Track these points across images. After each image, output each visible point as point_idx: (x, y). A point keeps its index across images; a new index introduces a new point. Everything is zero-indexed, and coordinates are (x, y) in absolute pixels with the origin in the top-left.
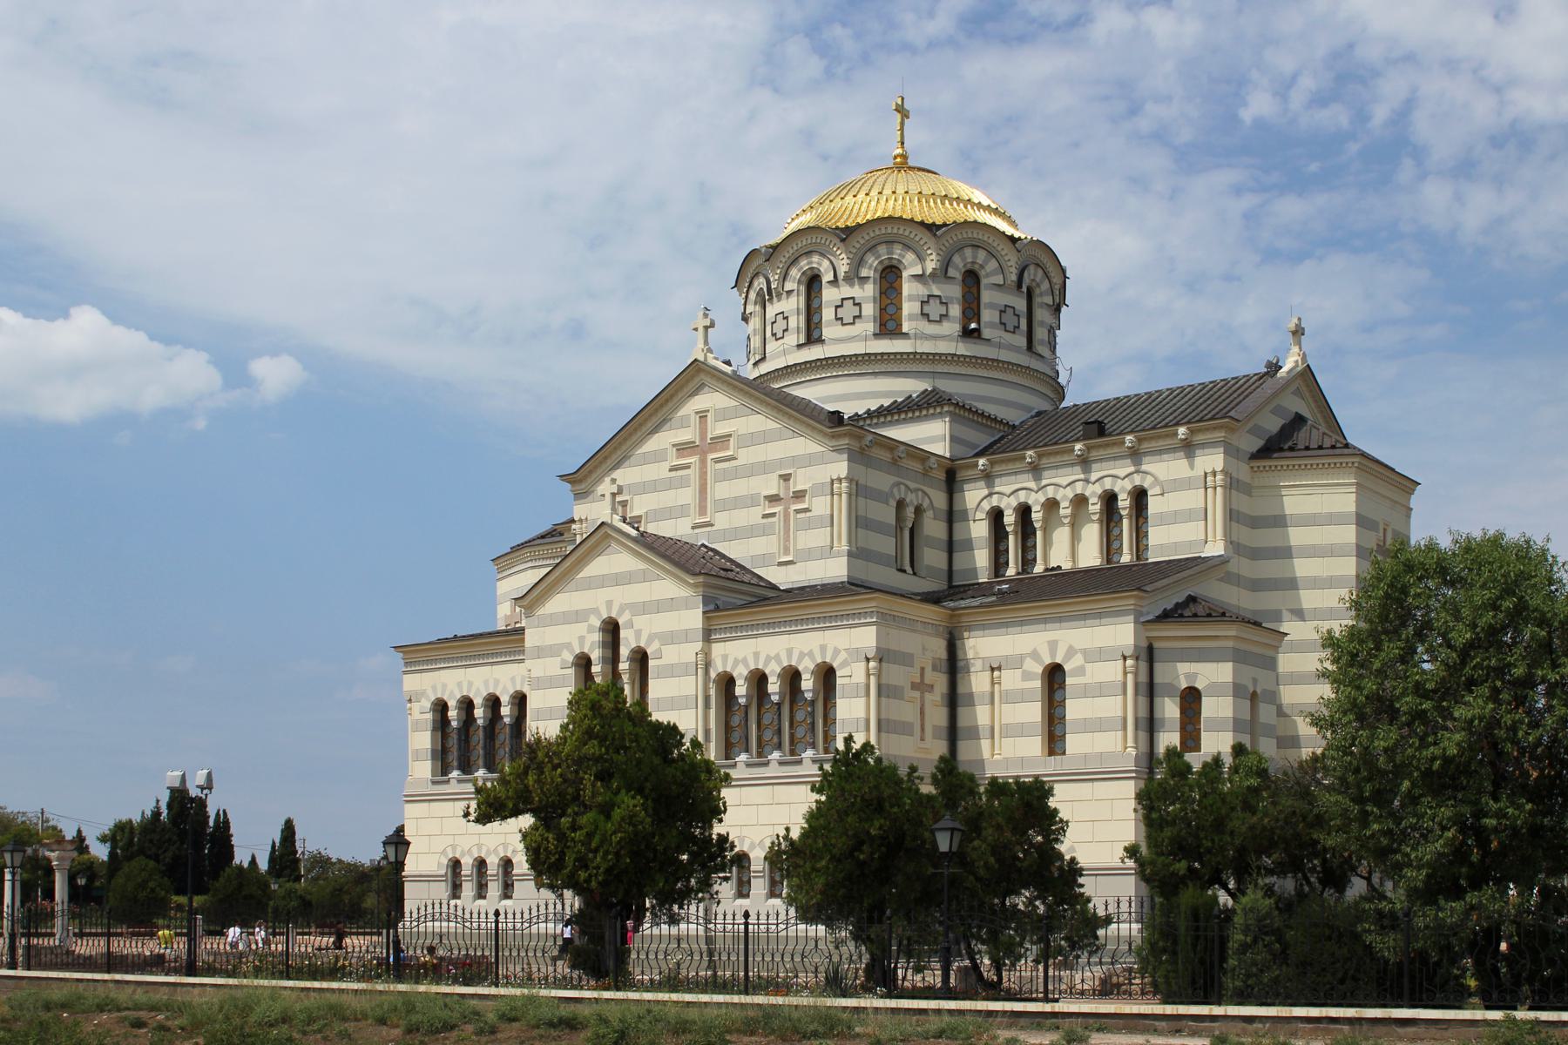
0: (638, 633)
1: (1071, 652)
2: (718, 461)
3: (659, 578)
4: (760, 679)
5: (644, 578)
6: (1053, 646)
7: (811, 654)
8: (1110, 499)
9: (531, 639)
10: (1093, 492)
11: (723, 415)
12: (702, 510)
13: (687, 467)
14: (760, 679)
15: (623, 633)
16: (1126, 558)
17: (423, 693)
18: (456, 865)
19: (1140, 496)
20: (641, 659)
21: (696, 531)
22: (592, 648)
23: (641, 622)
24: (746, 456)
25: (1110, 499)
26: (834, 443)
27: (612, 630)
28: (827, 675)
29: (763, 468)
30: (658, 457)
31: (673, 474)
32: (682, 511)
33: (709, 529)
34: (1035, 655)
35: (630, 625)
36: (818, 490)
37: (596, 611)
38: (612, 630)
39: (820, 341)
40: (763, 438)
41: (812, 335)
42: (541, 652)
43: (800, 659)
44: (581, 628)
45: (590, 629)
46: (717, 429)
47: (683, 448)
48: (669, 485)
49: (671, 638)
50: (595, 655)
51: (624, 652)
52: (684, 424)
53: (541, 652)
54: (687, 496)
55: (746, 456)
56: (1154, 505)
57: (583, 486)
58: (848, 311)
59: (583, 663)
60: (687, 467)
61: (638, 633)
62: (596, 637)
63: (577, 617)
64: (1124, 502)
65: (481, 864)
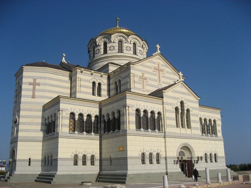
0: (188, 105)
5: (188, 94)
9: (165, 99)
11: (162, 65)
12: (160, 82)
15: (185, 105)
18: (143, 154)
20: (188, 111)
21: (159, 85)
23: (188, 103)
24: (167, 75)
27: (182, 103)
32: (155, 81)
33: (161, 86)
35: (186, 103)
38: (182, 103)
39: (122, 52)
40: (170, 73)
41: (121, 50)
42: (168, 104)
46: (161, 67)
48: (153, 74)
49: (194, 108)
50: (180, 108)
51: (186, 109)
52: (155, 63)
53: (168, 104)
54: (156, 78)
55: (167, 75)
57: (133, 66)
59: (177, 109)
61: (188, 105)
63: (175, 98)
65: (151, 154)
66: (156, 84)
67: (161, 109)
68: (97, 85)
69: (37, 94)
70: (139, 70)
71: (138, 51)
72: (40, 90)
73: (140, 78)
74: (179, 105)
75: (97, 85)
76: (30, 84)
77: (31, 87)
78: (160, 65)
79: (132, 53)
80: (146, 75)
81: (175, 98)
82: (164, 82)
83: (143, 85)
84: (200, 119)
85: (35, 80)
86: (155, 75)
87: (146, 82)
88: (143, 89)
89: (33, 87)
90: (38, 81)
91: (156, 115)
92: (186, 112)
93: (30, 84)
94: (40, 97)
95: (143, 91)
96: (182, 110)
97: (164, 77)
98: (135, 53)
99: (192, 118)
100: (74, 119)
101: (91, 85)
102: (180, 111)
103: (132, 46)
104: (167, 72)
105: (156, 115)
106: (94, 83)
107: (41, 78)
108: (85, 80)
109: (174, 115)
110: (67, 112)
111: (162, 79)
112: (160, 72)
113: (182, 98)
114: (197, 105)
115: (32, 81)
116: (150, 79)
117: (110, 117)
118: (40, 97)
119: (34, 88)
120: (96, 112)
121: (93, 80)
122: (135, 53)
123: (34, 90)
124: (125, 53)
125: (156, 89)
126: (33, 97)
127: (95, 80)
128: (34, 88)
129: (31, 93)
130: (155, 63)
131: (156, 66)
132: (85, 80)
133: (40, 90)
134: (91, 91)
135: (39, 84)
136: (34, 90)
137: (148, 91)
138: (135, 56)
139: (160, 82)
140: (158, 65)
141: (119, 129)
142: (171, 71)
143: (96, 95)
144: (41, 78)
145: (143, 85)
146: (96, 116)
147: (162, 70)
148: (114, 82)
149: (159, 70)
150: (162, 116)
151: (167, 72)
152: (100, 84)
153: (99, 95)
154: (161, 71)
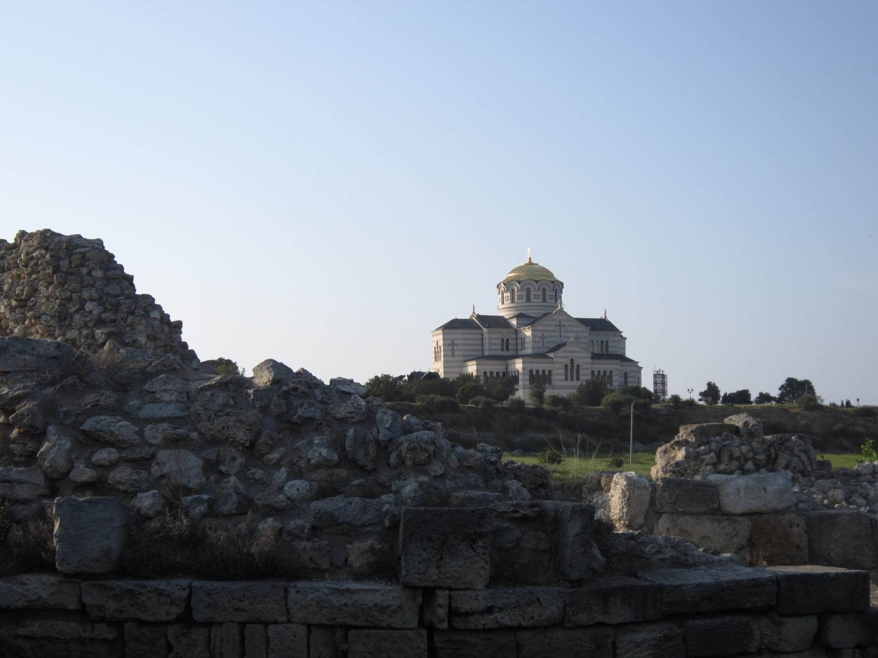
1: (628, 371)
5: (579, 352)
6: (626, 369)
8: (602, 342)
9: (555, 360)
10: (600, 340)
11: (564, 320)
12: (560, 337)
15: (575, 361)
16: (605, 352)
17: (527, 368)
19: (607, 342)
20: (578, 366)
25: (602, 342)
27: (572, 361)
28: (611, 372)
29: (572, 332)
30: (551, 325)
34: (623, 371)
36: (584, 337)
38: (572, 361)
42: (558, 363)
44: (567, 359)
46: (563, 323)
47: (556, 326)
48: (553, 331)
50: (570, 364)
51: (575, 365)
53: (558, 363)
54: (557, 334)
55: (569, 329)
56: (610, 344)
59: (566, 366)
62: (570, 361)
64: (605, 343)
66: (556, 340)
68: (505, 341)
69: (456, 353)
71: (547, 297)
73: (540, 337)
74: (569, 363)
76: (449, 345)
77: (450, 348)
78: (562, 321)
79: (541, 300)
80: (546, 334)
82: (564, 337)
84: (593, 372)
85: (453, 341)
86: (556, 331)
88: (543, 346)
90: (456, 342)
91: (547, 373)
92: (575, 367)
93: (449, 345)
97: (564, 331)
98: (544, 300)
99: (581, 372)
100: (486, 376)
101: (500, 342)
102: (569, 367)
103: (540, 293)
105: (547, 373)
106: (502, 339)
107: (457, 339)
108: (494, 339)
109: (563, 371)
110: (482, 372)
111: (563, 334)
112: (562, 328)
114: (589, 360)
115: (450, 342)
116: (550, 337)
117: (513, 374)
119: (453, 348)
120: (503, 369)
121: (502, 337)
122: (544, 300)
125: (557, 344)
126: (453, 356)
127: (503, 337)
128: (453, 348)
129: (450, 353)
130: (556, 320)
131: (557, 323)
132: (494, 339)
134: (500, 347)
135: (456, 345)
136: (453, 350)
138: (544, 304)
139: (560, 337)
140: (560, 321)
141: (518, 384)
144: (457, 339)
146: (504, 373)
147: (564, 326)
149: (560, 326)
152: (508, 340)
153: (508, 350)
154: (562, 326)
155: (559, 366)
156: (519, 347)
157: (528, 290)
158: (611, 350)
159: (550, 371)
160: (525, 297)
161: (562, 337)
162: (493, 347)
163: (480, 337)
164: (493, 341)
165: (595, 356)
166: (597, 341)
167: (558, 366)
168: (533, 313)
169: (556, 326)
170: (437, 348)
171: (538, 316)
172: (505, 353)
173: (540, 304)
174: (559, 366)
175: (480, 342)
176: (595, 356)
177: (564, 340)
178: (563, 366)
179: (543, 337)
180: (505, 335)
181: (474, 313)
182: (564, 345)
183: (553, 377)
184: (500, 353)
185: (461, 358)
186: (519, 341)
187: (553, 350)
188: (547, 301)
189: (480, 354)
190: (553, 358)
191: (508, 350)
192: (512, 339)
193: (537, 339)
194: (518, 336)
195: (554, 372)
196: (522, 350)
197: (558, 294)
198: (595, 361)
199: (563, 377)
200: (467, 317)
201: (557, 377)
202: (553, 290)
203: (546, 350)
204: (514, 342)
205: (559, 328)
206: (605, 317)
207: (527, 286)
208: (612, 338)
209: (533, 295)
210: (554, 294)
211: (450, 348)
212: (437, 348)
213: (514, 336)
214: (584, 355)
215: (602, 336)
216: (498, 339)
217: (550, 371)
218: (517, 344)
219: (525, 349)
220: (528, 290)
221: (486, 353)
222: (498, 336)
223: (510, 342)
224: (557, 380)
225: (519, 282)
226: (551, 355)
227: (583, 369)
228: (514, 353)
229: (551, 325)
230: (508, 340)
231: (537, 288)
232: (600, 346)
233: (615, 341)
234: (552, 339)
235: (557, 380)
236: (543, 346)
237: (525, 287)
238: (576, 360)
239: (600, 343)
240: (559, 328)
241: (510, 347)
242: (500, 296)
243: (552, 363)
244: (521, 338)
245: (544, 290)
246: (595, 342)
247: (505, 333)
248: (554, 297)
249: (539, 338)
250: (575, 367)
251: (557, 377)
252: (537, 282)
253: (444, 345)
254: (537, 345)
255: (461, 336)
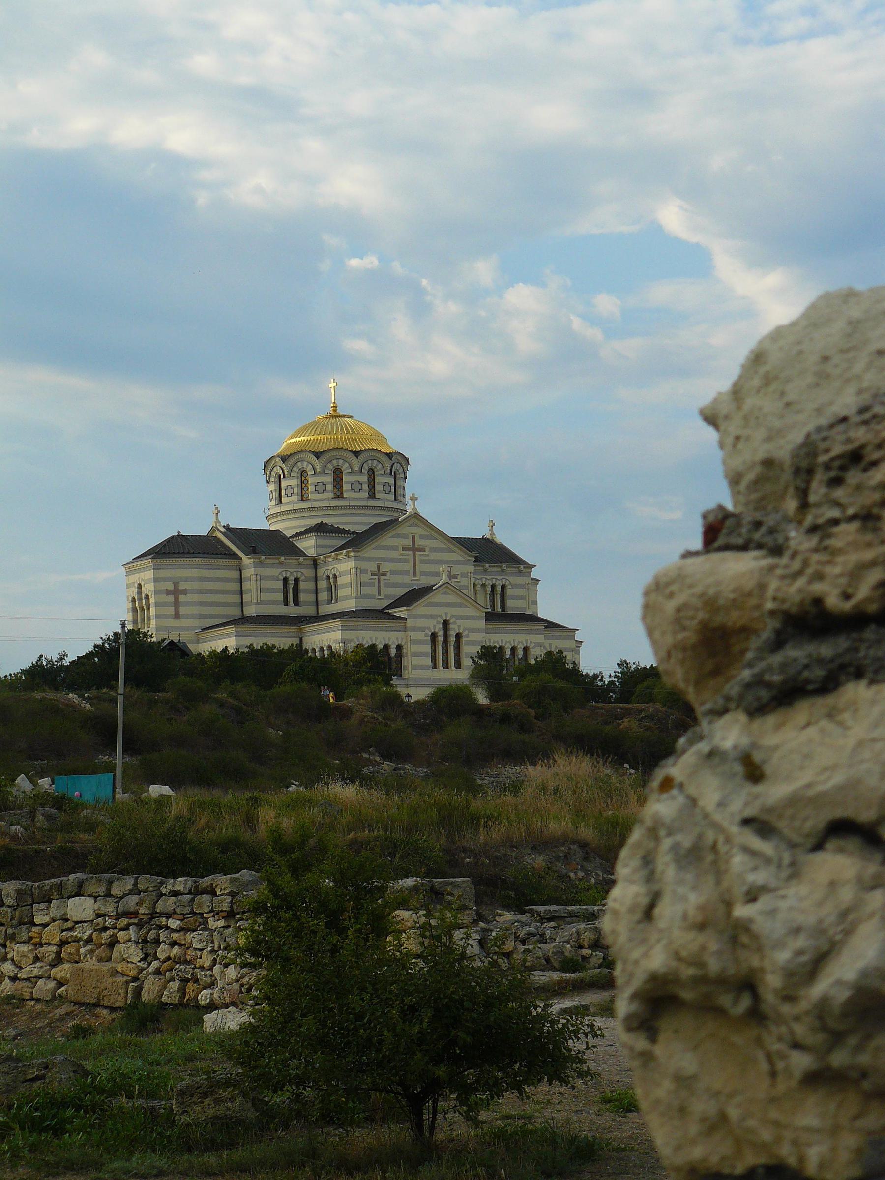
0: (459, 627)
2: (421, 555)
3: (466, 606)
4: (513, 649)
5: (460, 605)
7: (522, 642)
8: (493, 587)
9: (410, 623)
11: (422, 537)
12: (415, 575)
13: (408, 555)
14: (513, 649)
15: (451, 626)
16: (499, 610)
19: (503, 587)
20: (458, 636)
21: (413, 582)
22: (439, 630)
23: (459, 622)
25: (493, 587)
26: (469, 558)
27: (446, 624)
30: (395, 548)
31: (401, 557)
32: (406, 573)
35: (455, 623)
36: (464, 575)
37: (440, 616)
38: (446, 624)
42: (415, 629)
43: (506, 644)
44: (434, 622)
45: (438, 623)
46: (419, 543)
47: (404, 549)
48: (399, 561)
49: (473, 630)
50: (441, 633)
51: (452, 633)
52: (405, 536)
53: (415, 629)
54: (409, 567)
56: (509, 591)
58: (387, 488)
59: (434, 636)
60: (408, 555)
61: (459, 627)
63: (432, 617)
64: (499, 589)
66: (407, 579)
67: (402, 639)
68: (291, 583)
69: (183, 610)
70: (370, 559)
71: (379, 488)
72: (188, 604)
75: (291, 583)
76: (168, 592)
77: (171, 599)
80: (386, 567)
81: (432, 617)
82: (423, 574)
83: (379, 586)
85: (176, 584)
86: (406, 561)
87: (386, 581)
88: (379, 594)
89: (175, 598)
90: (181, 588)
92: (452, 639)
93: (168, 592)
94: (188, 616)
95: (378, 599)
96: (446, 635)
97: (422, 562)
98: (372, 495)
101: (280, 585)
102: (440, 639)
103: (364, 479)
104: (434, 550)
106: (285, 580)
107: (186, 579)
109: (428, 648)
111: (420, 567)
113: (446, 613)
114: (482, 624)
116: (394, 573)
118: (188, 616)
122: (372, 495)
123: (177, 604)
124: (349, 499)
126: (177, 616)
129: (171, 610)
131: (408, 542)
133: (188, 604)
134: (280, 597)
135: (185, 592)
136: (177, 604)
137: (387, 597)
138: (371, 503)
139: (415, 574)
140: (413, 538)
142: (443, 546)
143: (291, 603)
144: (186, 579)
145: (379, 586)
148: (325, 576)
149: (414, 549)
150: (404, 651)
151: (434, 550)
152: (297, 580)
153: (296, 603)
155: (420, 636)
156: (323, 596)
157: (338, 474)
158: (513, 605)
159: (399, 648)
160: (330, 487)
161: (418, 574)
162: (266, 597)
163: (235, 574)
164: (265, 584)
165: (491, 617)
166: (483, 585)
167: (414, 635)
168: (350, 523)
169: (404, 549)
170: (140, 599)
171: (360, 529)
172: (292, 610)
173: (364, 503)
174: (420, 636)
175: (235, 586)
176: (491, 617)
177: (425, 581)
178: (426, 635)
179: (379, 573)
180: (292, 570)
181: (217, 521)
182: (426, 590)
183: (405, 662)
184: (282, 610)
185: (197, 623)
186: (323, 584)
187: (402, 601)
188: (377, 496)
189: (236, 612)
190: (405, 619)
191: (296, 603)
192: (307, 579)
193: (365, 578)
194: (321, 572)
195: (409, 649)
196: (329, 602)
197: (400, 483)
198: (494, 626)
199: (428, 661)
200: (203, 531)
201: (416, 661)
202: (391, 474)
203: (387, 602)
204: (311, 585)
205: (411, 553)
206: (492, 534)
207: (335, 462)
208: (513, 579)
209: (347, 483)
210: (392, 481)
211: (171, 599)
212: (140, 599)
213: (309, 573)
214: (470, 611)
215: (495, 576)
216: (278, 579)
217: (399, 648)
218: (316, 591)
219: (336, 601)
220: (338, 474)
221: (251, 611)
222: (275, 572)
223: (302, 585)
224: (415, 667)
225: (318, 455)
226: (401, 612)
227: (468, 643)
228: (310, 611)
229: (395, 548)
230: (297, 580)
231: (357, 469)
232: (488, 596)
233: (521, 586)
234: (398, 579)
235: (415, 667)
236: (379, 594)
237: (330, 466)
238: (455, 623)
239: (489, 589)
240: (411, 553)
241: (302, 597)
242: (272, 487)
243: (405, 630)
244: (328, 577)
245: (372, 471)
246: (479, 587)
247: (291, 569)
248: (393, 490)
249: (369, 576)
250: (452, 639)
251: (416, 661)
252: (356, 454)
253: (157, 592)
254: (366, 590)
255: (195, 573)
